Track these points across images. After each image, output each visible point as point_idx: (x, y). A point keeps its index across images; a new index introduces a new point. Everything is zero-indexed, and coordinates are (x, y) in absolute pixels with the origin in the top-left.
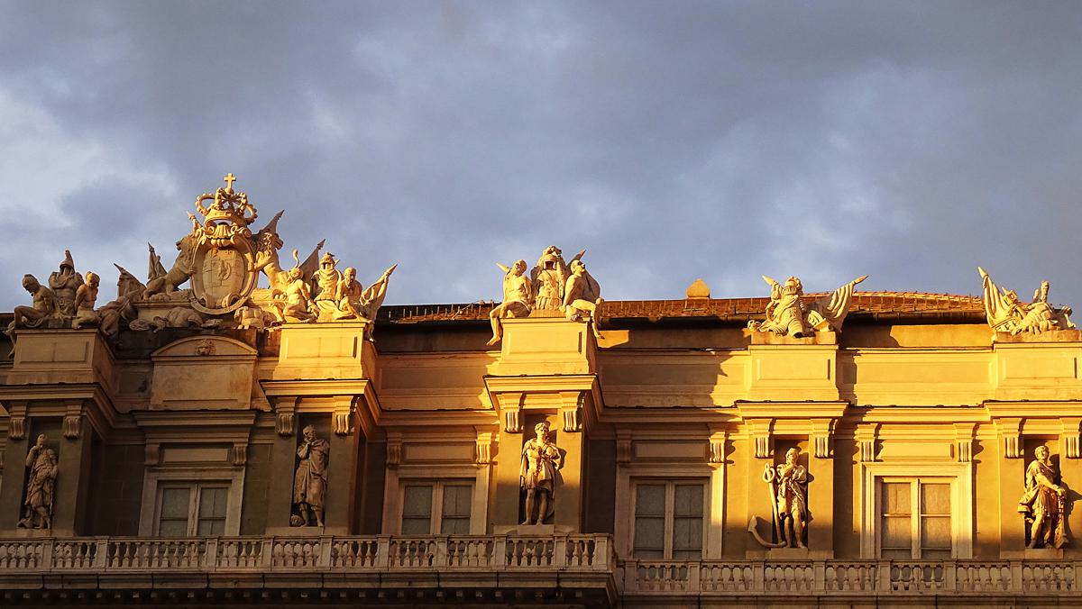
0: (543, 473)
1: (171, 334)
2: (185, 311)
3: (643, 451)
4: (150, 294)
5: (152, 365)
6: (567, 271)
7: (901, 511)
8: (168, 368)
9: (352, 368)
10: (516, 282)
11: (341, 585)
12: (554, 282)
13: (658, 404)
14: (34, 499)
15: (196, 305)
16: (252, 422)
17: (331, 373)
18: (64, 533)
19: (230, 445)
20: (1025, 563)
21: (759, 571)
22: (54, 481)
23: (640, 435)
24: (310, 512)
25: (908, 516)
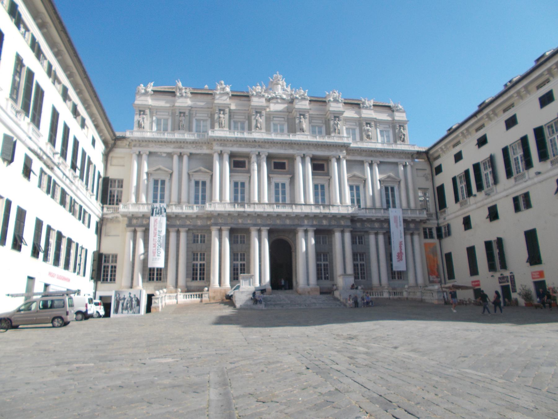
1: (273, 98)
14: (259, 125)
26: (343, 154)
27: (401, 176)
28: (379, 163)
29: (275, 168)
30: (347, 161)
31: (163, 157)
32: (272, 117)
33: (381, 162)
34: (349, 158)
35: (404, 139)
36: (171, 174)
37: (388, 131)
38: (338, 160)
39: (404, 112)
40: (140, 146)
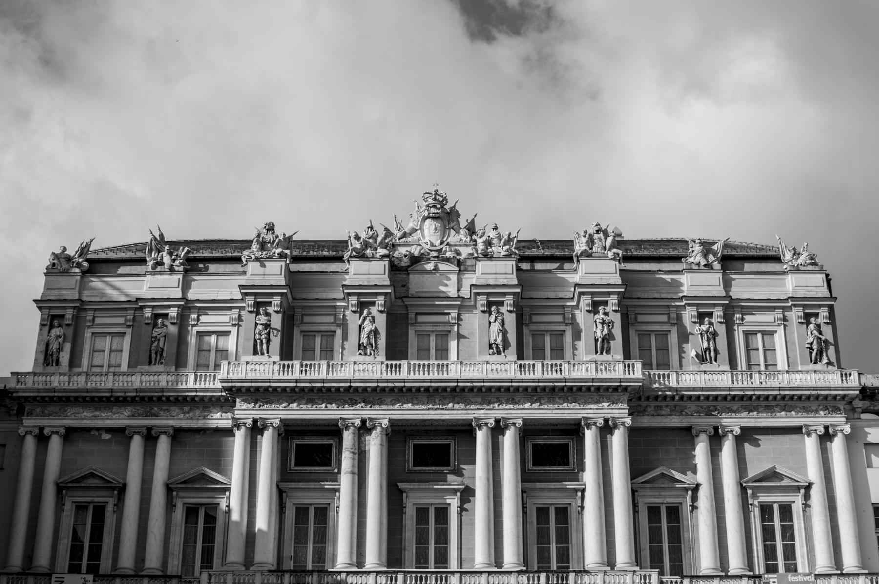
0: (605, 330)
2: (419, 248)
3: (641, 318)
4: (399, 239)
5: (408, 274)
6: (606, 235)
7: (755, 347)
8: (416, 276)
9: (512, 279)
10: (584, 240)
11: (521, 384)
12: (600, 240)
13: (646, 296)
14: (364, 341)
15: (424, 245)
16: (459, 303)
17: (496, 279)
18: (381, 357)
19: (449, 314)
20: (815, 372)
21: (703, 375)
22: (376, 332)
23: (638, 311)
24: (497, 347)
25: (757, 349)
26: (620, 412)
27: (813, 473)
28: (739, 431)
29: (414, 465)
30: (633, 434)
31: (105, 441)
32: (412, 315)
33: (743, 429)
34: (646, 421)
35: (820, 353)
36: (122, 490)
37: (772, 333)
38: (606, 429)
39: (822, 270)
40: (43, 415)
